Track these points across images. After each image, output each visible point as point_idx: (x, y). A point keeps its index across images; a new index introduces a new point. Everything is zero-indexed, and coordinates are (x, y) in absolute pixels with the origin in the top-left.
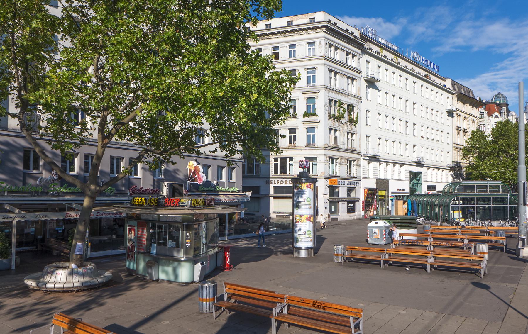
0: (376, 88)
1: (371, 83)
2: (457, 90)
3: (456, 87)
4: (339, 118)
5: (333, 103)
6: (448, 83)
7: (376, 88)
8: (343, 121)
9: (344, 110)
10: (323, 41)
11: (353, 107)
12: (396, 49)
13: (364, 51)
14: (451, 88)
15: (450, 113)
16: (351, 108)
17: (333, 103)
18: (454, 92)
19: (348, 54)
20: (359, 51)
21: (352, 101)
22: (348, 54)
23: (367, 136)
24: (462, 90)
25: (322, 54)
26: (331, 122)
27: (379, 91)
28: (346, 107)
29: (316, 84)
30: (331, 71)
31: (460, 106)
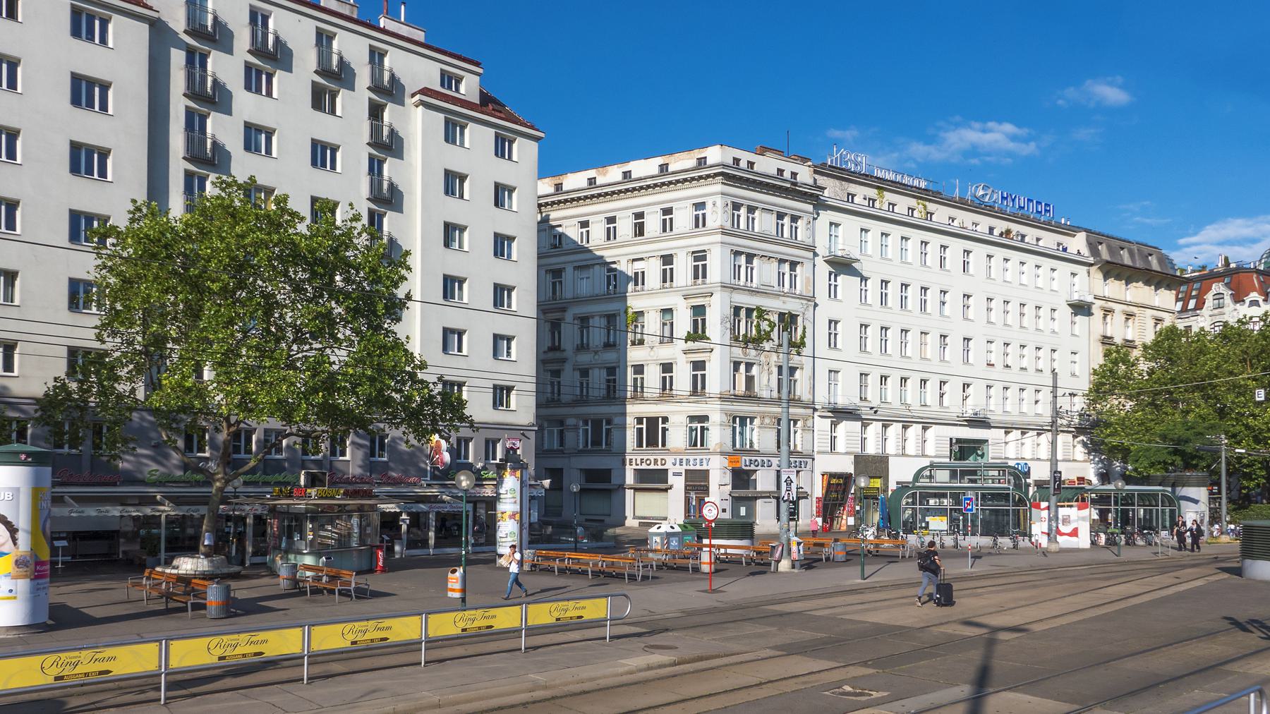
0: (855, 273)
1: (842, 266)
2: (1105, 255)
3: (1103, 249)
4: (756, 341)
5: (743, 313)
6: (1077, 244)
7: (855, 273)
8: (767, 345)
9: (772, 325)
10: (719, 200)
11: (793, 318)
12: (923, 185)
13: (820, 205)
14: (1085, 251)
15: (1081, 308)
16: (788, 320)
17: (743, 313)
18: (1091, 260)
19: (780, 216)
20: (810, 208)
21: (791, 306)
22: (780, 216)
23: (830, 374)
24: (1125, 253)
25: (718, 224)
26: (738, 352)
27: (864, 279)
28: (775, 318)
29: (708, 280)
30: (737, 254)
31: (1115, 288)
